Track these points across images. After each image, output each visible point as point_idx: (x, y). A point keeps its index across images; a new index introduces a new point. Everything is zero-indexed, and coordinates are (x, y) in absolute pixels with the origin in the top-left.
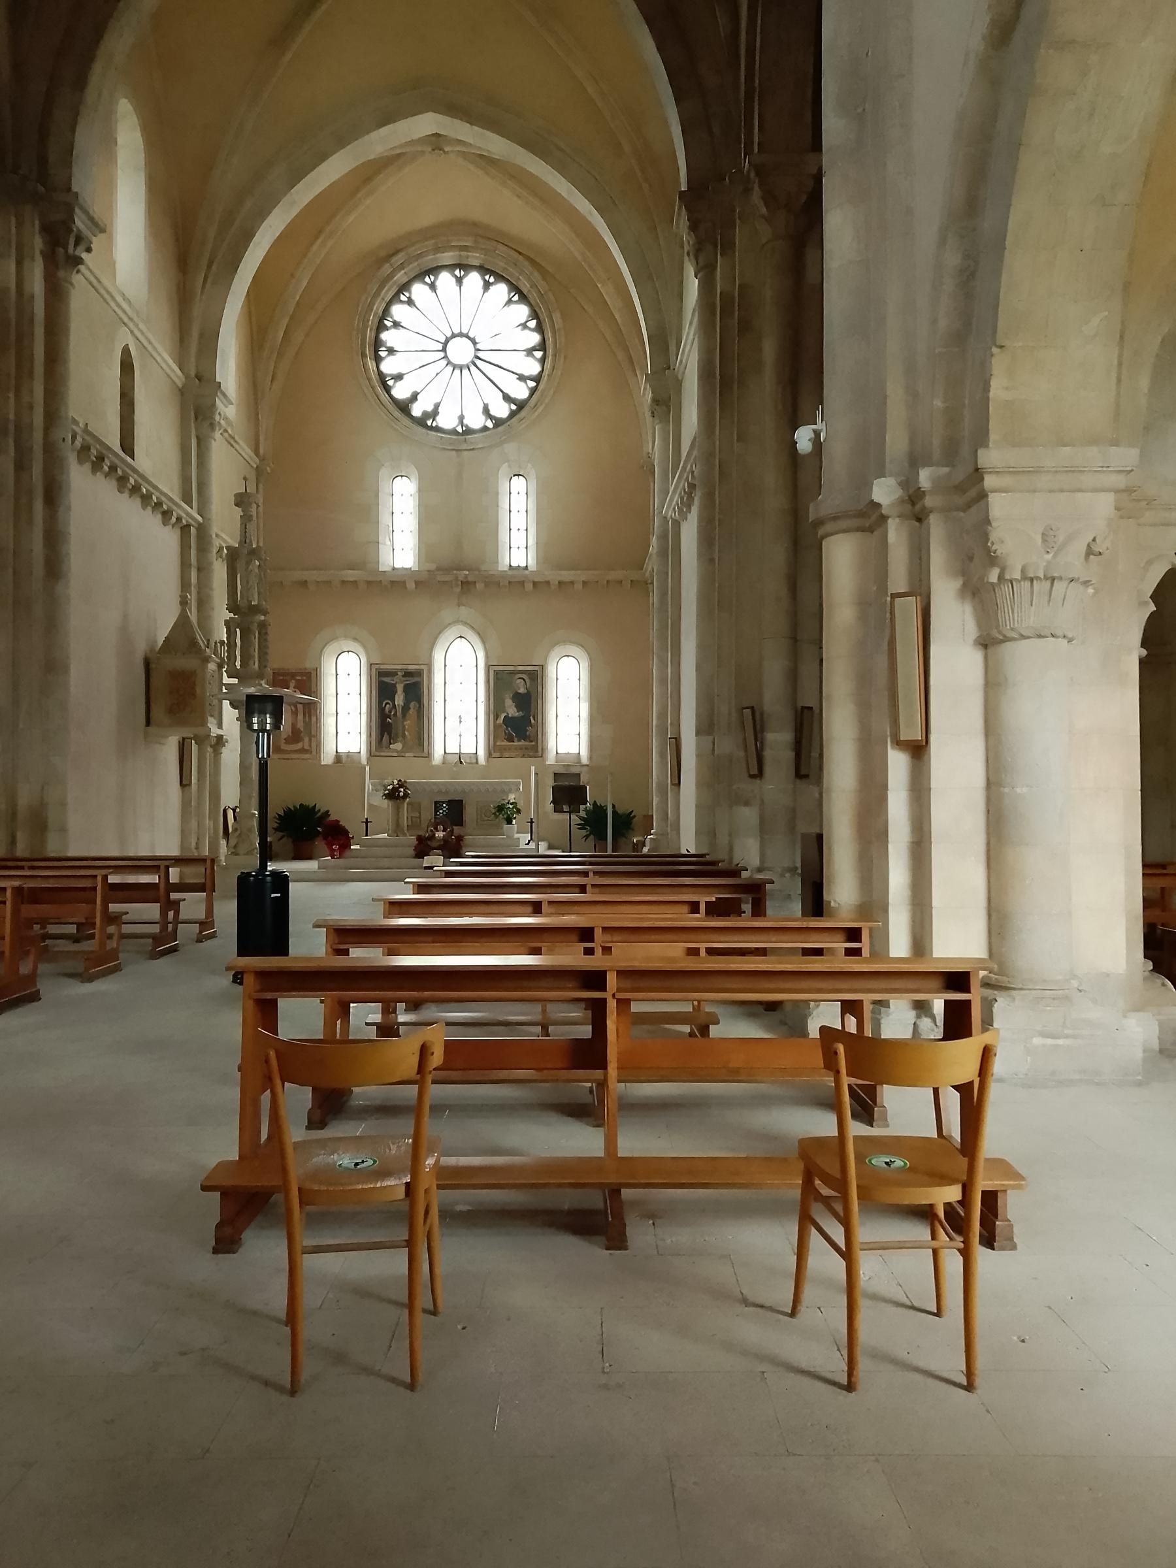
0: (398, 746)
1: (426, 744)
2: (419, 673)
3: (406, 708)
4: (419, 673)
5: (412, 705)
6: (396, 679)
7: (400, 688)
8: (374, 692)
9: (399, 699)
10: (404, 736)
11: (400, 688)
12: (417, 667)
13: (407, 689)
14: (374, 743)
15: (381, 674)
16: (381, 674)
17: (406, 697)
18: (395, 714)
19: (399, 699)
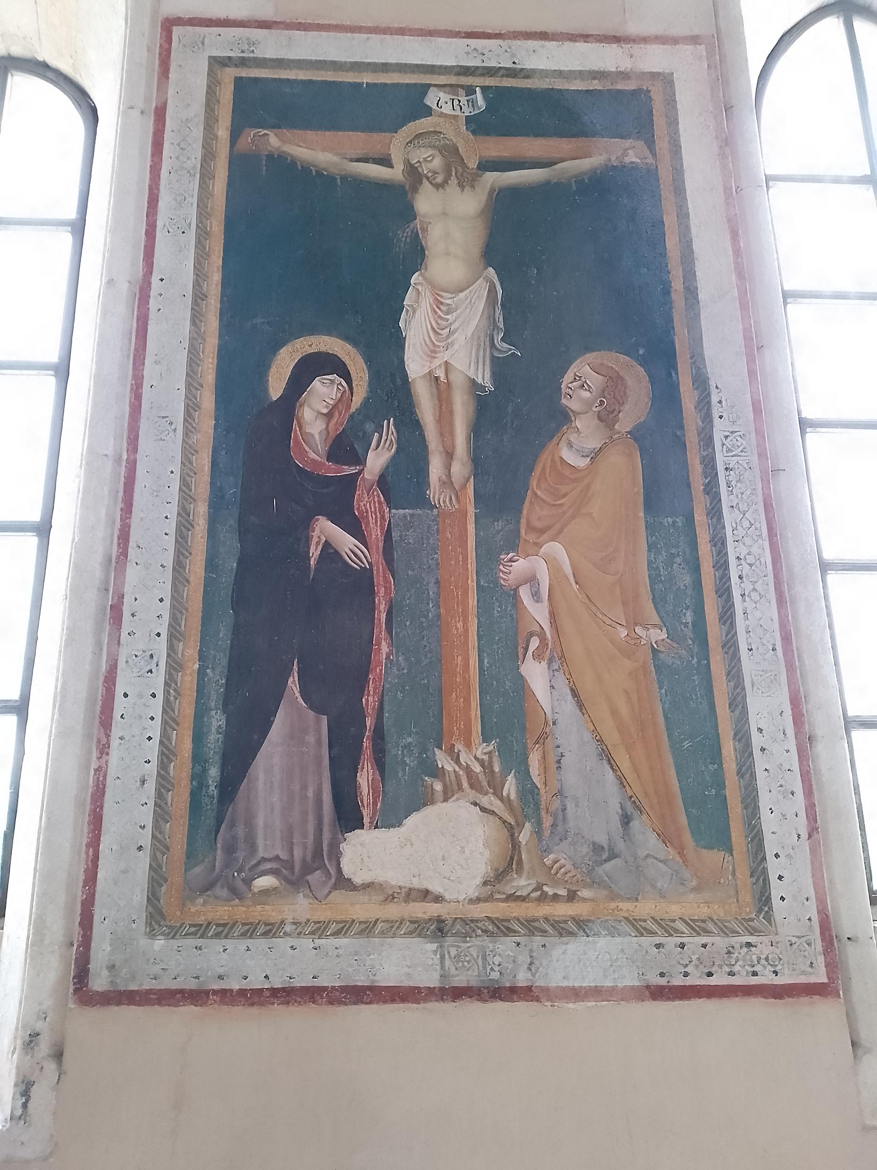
0: (436, 848)
1: (780, 819)
2: (633, 108)
3: (515, 415)
4: (633, 108)
5: (583, 380)
6: (402, 151)
7: (451, 224)
8: (177, 261)
9: (448, 331)
10: (511, 721)
11: (451, 224)
12: (608, 58)
13: (517, 236)
14: (131, 815)
15: (260, 99)
16: (260, 99)
17: (516, 311)
18: (406, 481)
19: (448, 331)
